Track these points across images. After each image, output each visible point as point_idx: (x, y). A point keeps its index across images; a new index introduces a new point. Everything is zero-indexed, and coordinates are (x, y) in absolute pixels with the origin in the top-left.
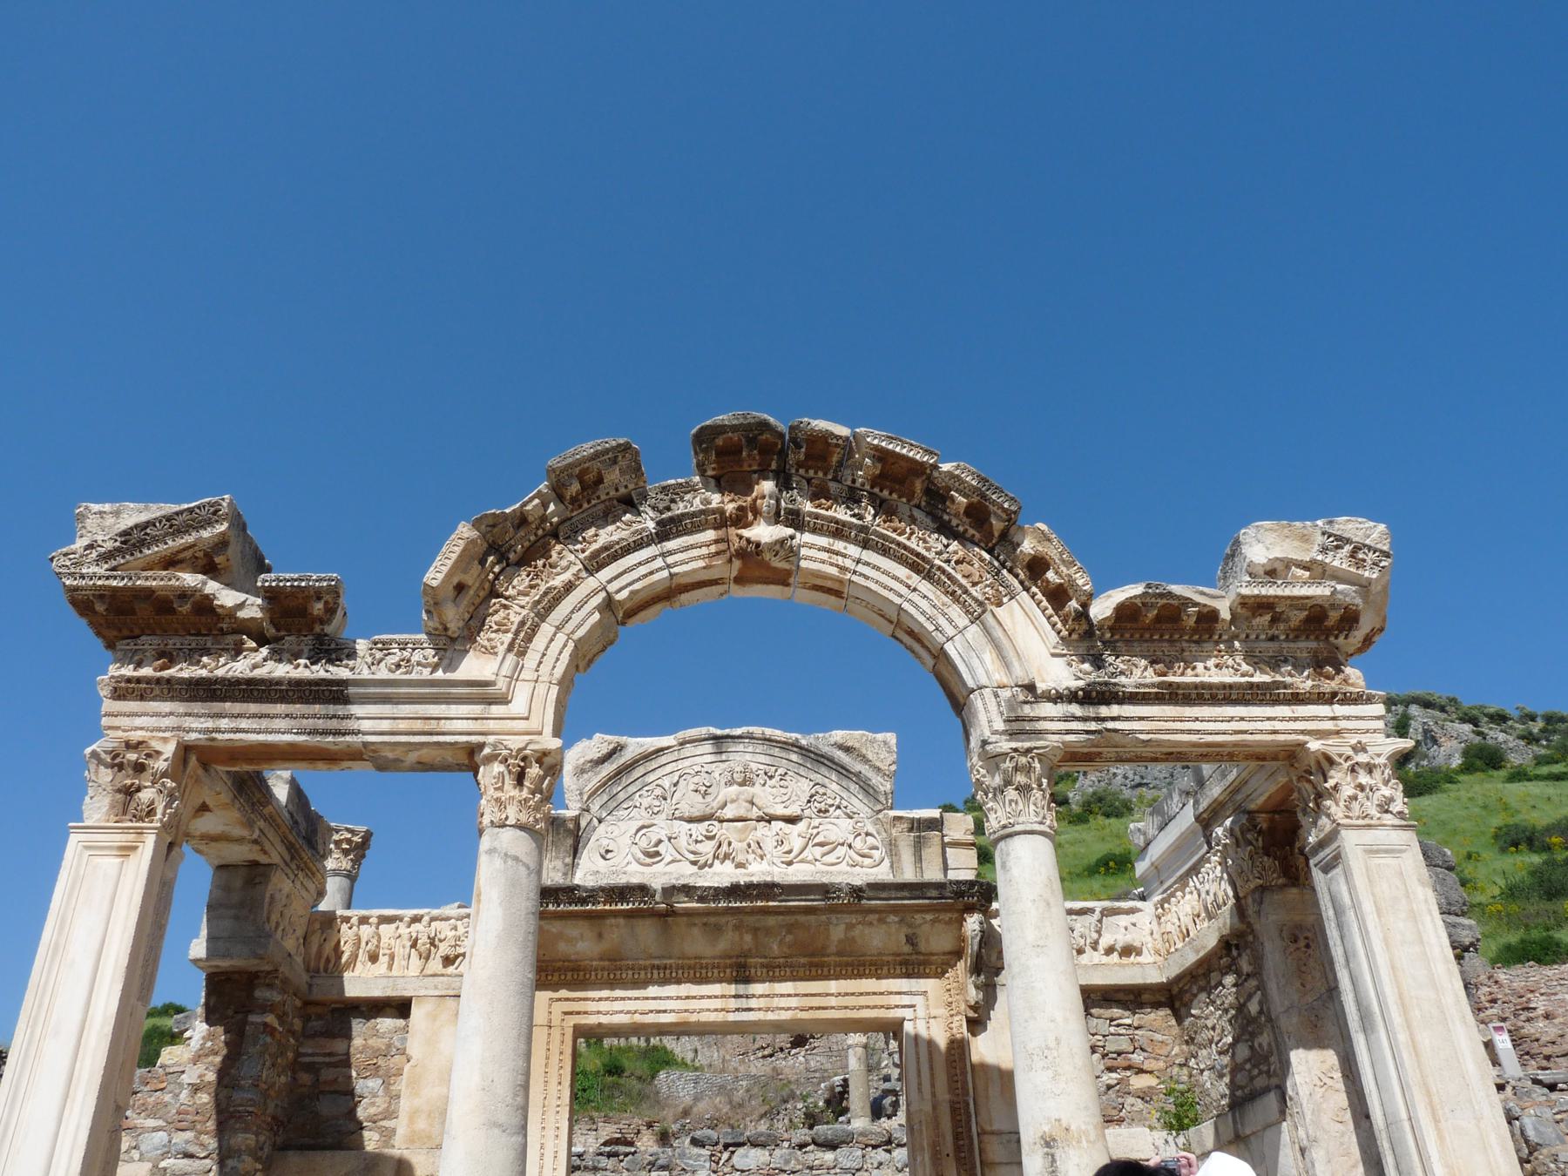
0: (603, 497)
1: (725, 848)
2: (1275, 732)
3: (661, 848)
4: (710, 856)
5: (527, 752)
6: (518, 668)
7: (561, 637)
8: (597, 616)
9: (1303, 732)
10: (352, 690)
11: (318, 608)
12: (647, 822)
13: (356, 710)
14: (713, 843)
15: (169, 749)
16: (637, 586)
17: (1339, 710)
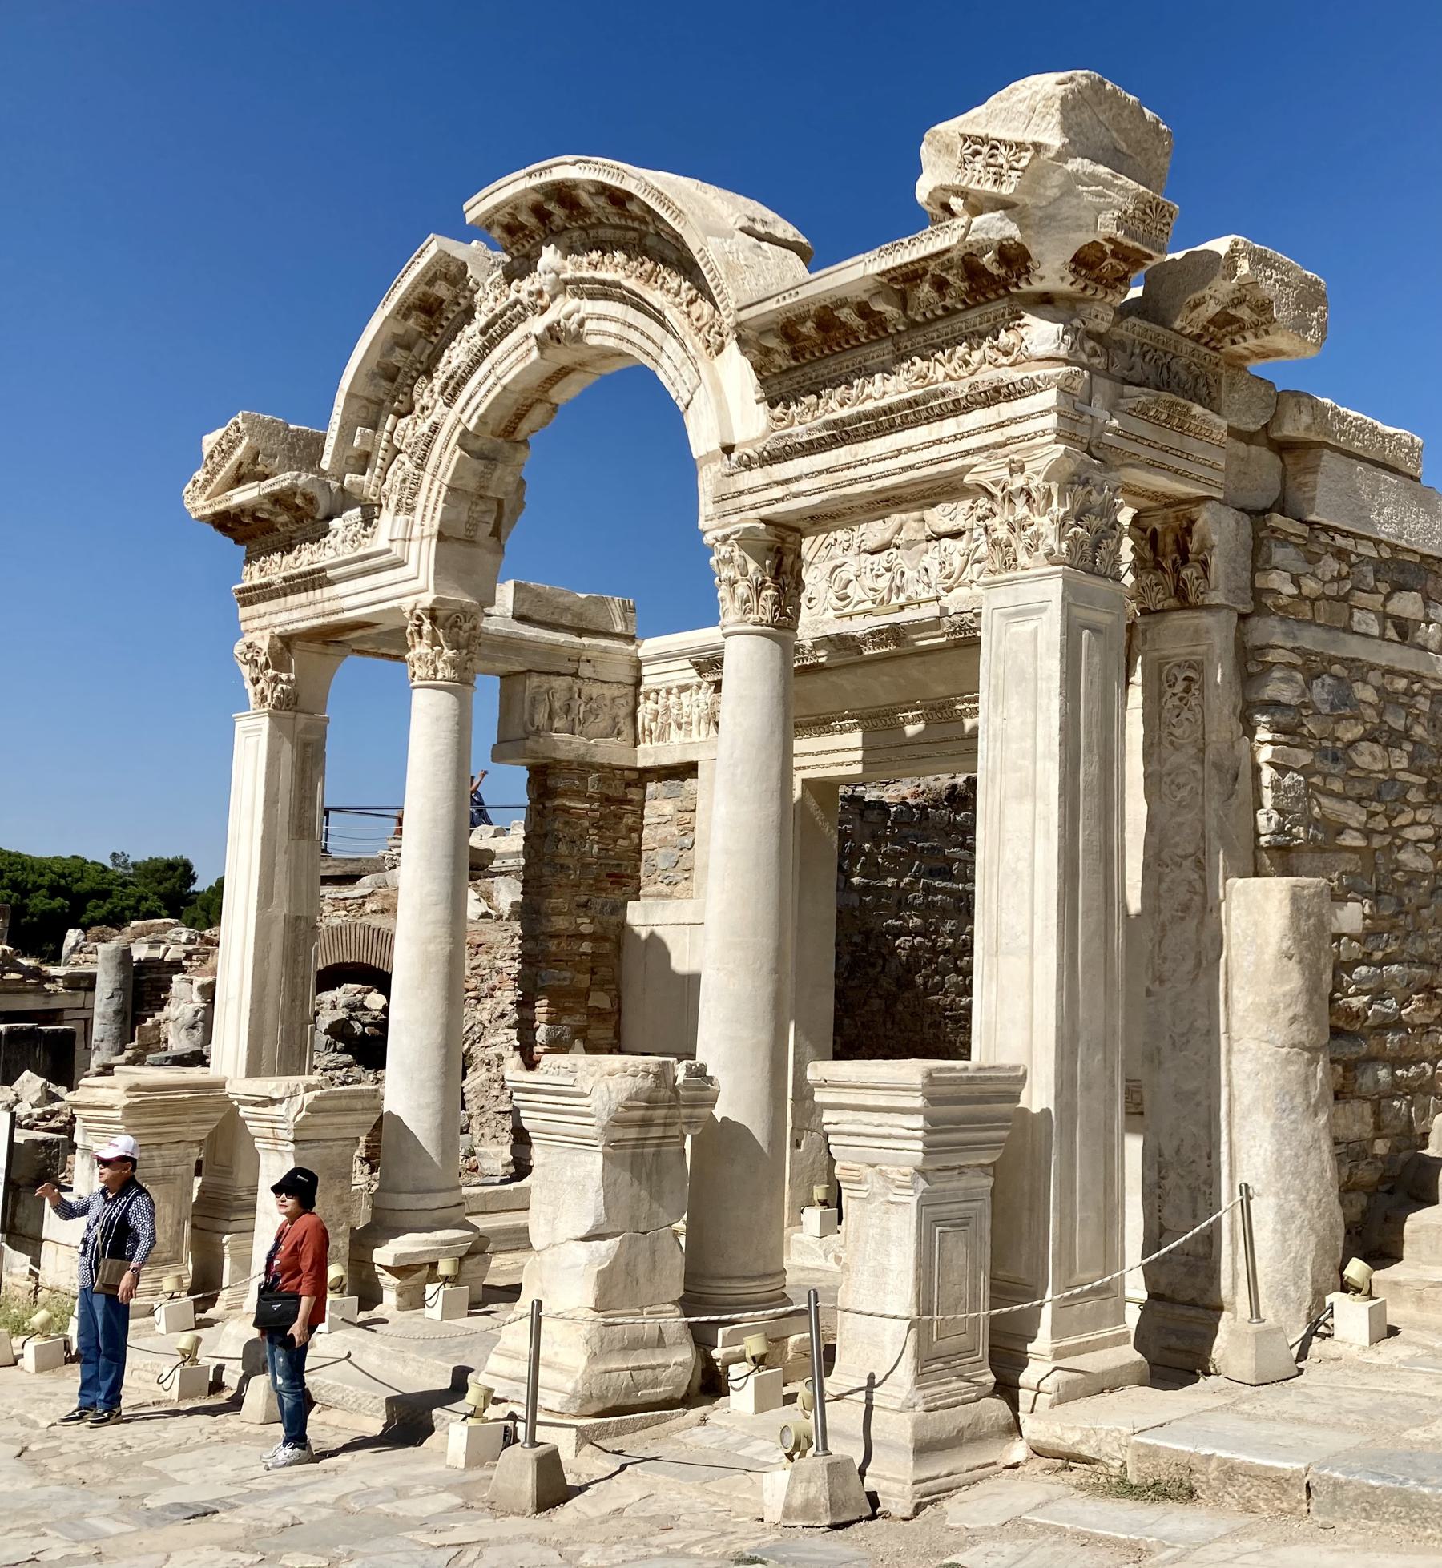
0: (451, 316)
1: (898, 581)
2: (940, 460)
3: (850, 591)
4: (886, 592)
5: (418, 612)
6: (409, 525)
7: (437, 483)
8: (458, 452)
9: (967, 453)
10: (330, 574)
11: (298, 501)
12: (838, 562)
13: (340, 589)
14: (889, 575)
15: (264, 645)
16: (481, 411)
17: (1005, 410)
